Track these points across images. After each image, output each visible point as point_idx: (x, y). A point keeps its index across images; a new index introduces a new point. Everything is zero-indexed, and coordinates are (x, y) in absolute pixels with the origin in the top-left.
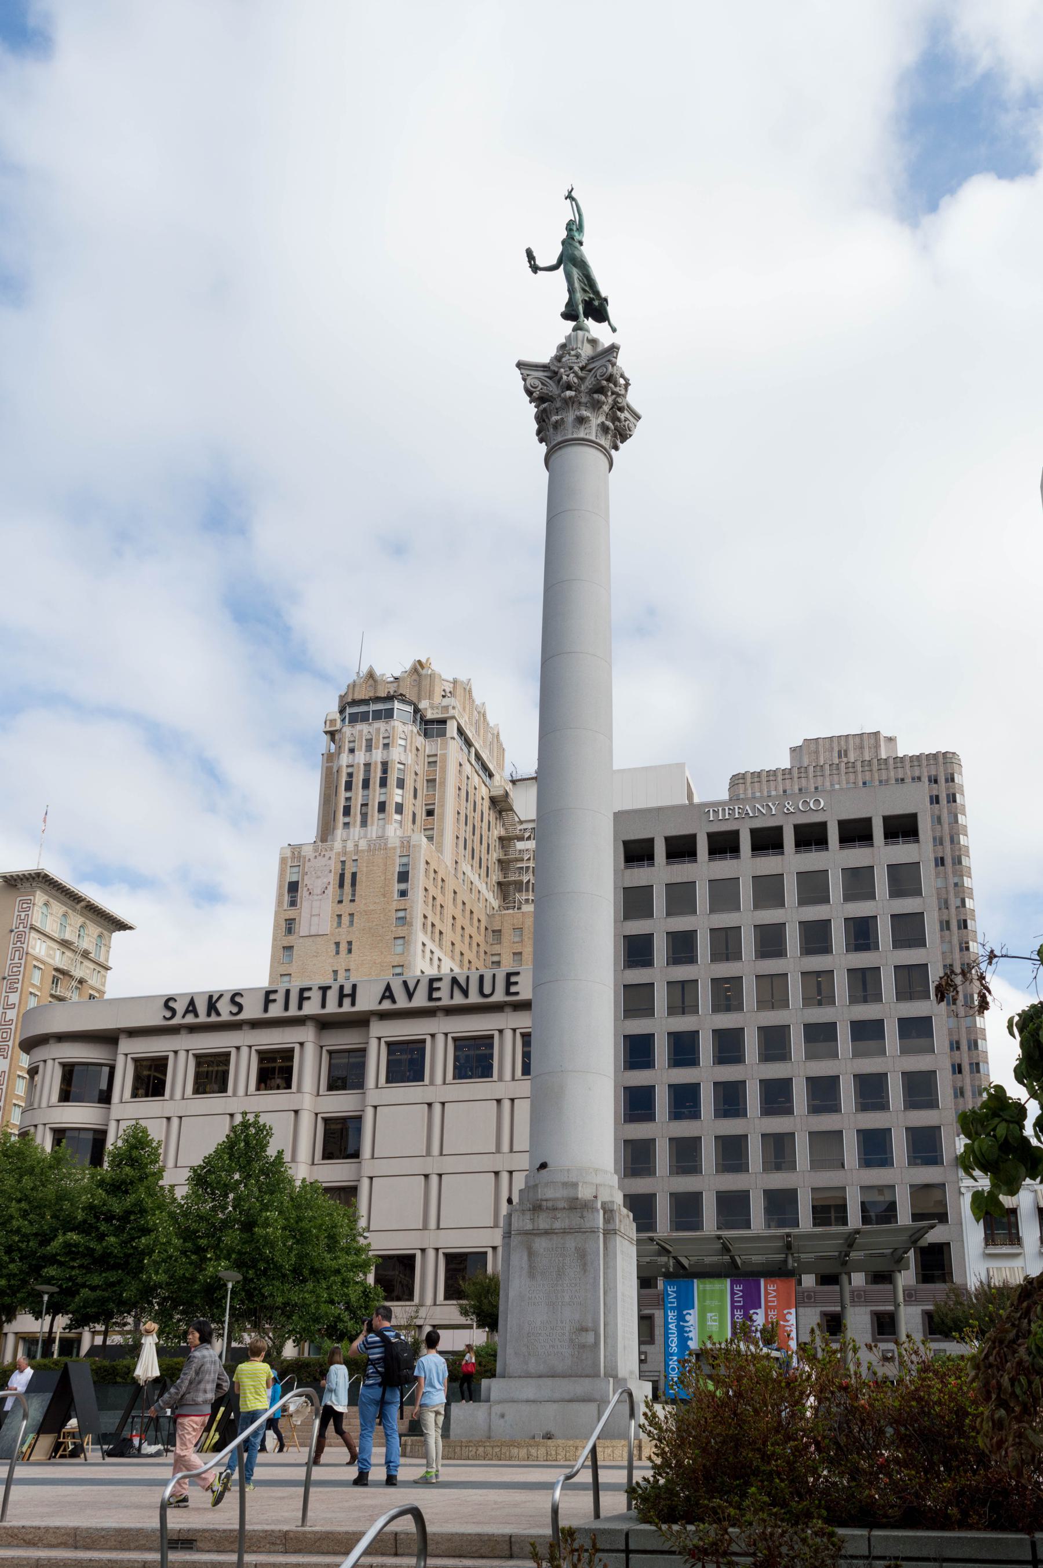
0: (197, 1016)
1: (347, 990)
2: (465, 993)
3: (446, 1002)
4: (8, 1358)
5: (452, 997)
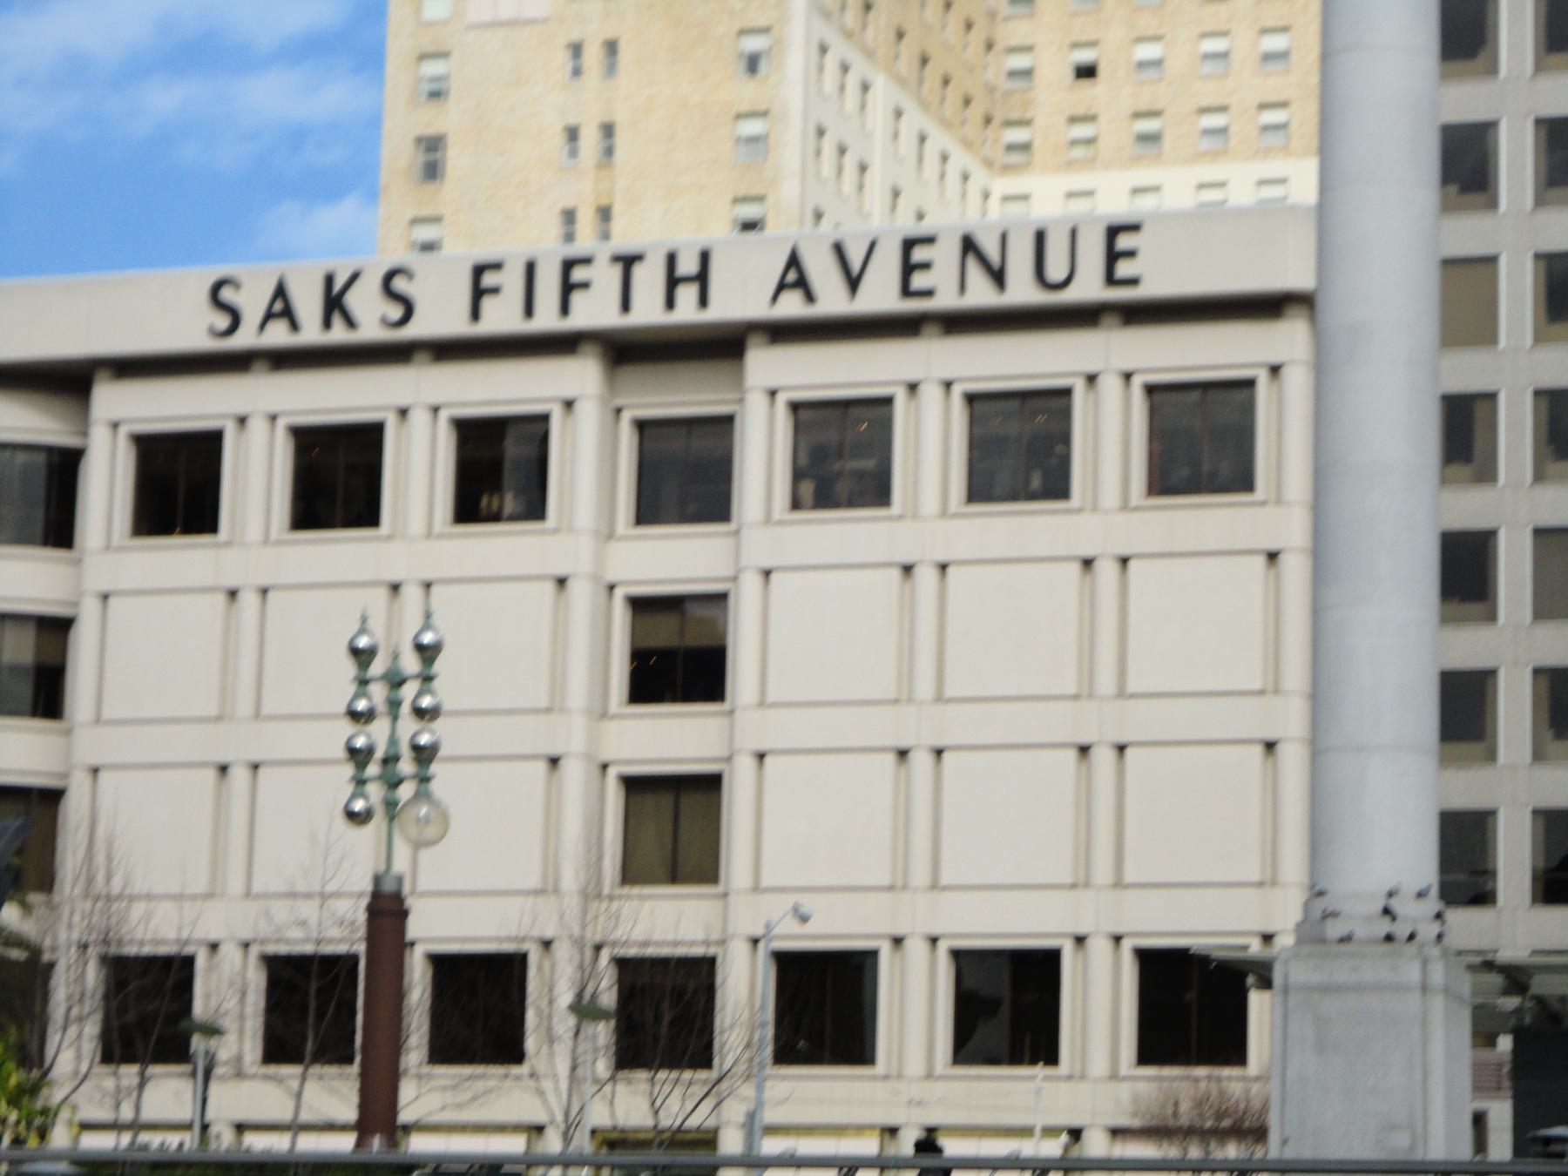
0: (294, 326)
1: (688, 266)
2: (998, 277)
3: (947, 299)
4: (63, 1167)
5: (962, 287)
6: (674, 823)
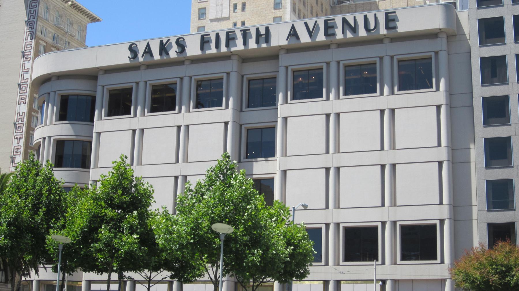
1: (263, 31)
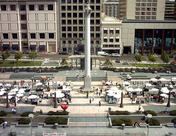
6: (24, 27)
